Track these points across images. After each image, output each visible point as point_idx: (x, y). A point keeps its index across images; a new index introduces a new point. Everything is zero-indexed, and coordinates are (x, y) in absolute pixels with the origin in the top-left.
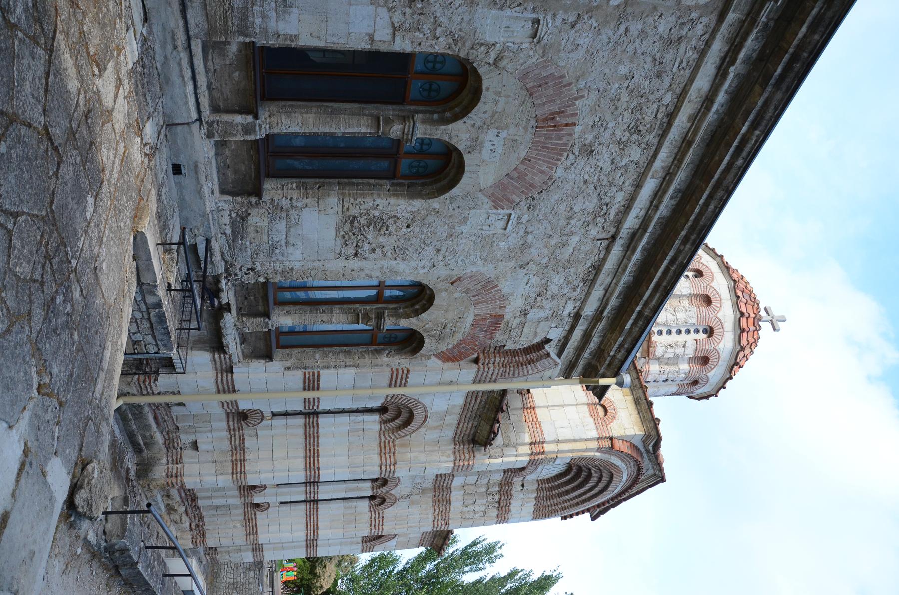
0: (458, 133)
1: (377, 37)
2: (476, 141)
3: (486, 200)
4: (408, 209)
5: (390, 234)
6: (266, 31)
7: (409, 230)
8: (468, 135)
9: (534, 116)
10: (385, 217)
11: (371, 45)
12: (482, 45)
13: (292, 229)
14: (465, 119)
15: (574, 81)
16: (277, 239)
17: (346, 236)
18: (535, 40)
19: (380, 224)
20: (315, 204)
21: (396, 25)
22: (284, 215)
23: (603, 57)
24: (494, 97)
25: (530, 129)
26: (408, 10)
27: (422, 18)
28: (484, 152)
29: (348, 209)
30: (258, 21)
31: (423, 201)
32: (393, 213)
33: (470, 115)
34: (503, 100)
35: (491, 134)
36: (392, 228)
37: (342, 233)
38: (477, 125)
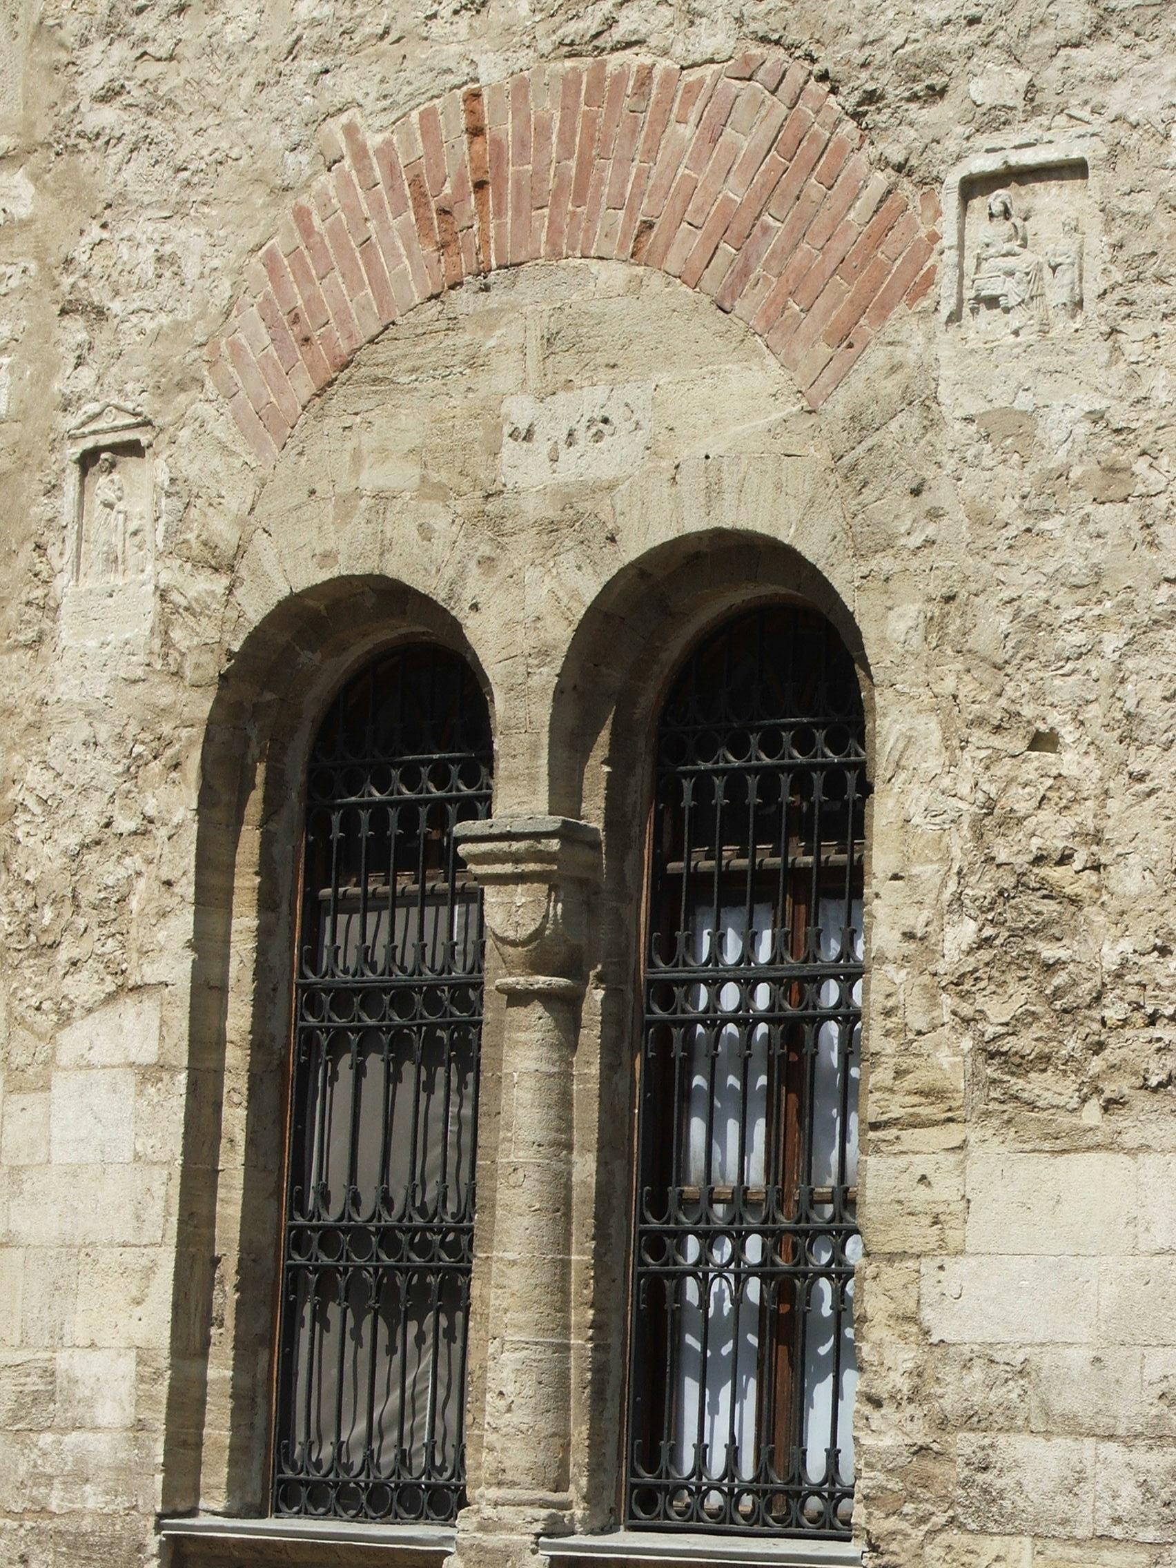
0: (519, 629)
1: (148, 1053)
2: (552, 527)
3: (877, 356)
4: (933, 764)
5: (1097, 838)
6: (122, 1469)
7: (1068, 734)
8: (531, 574)
9: (434, 308)
10: (982, 887)
11: (173, 1070)
12: (167, 643)
13: (1058, 1406)
14: (460, 612)
15: (289, 201)
16: (1129, 1493)
17: (1111, 1089)
18: (144, 437)
19: (1023, 909)
20: (893, 1275)
21: (110, 987)
22: (965, 1443)
23: (199, 132)
24: (358, 519)
25: (494, 299)
26: (63, 955)
27: (89, 894)
28: (607, 472)
29: (932, 1094)
30: (93, 1499)
31: (881, 699)
32: (959, 843)
33: (440, 596)
34: (370, 479)
35: (529, 474)
36: (1053, 831)
37: (1092, 1113)
38: (486, 550)
